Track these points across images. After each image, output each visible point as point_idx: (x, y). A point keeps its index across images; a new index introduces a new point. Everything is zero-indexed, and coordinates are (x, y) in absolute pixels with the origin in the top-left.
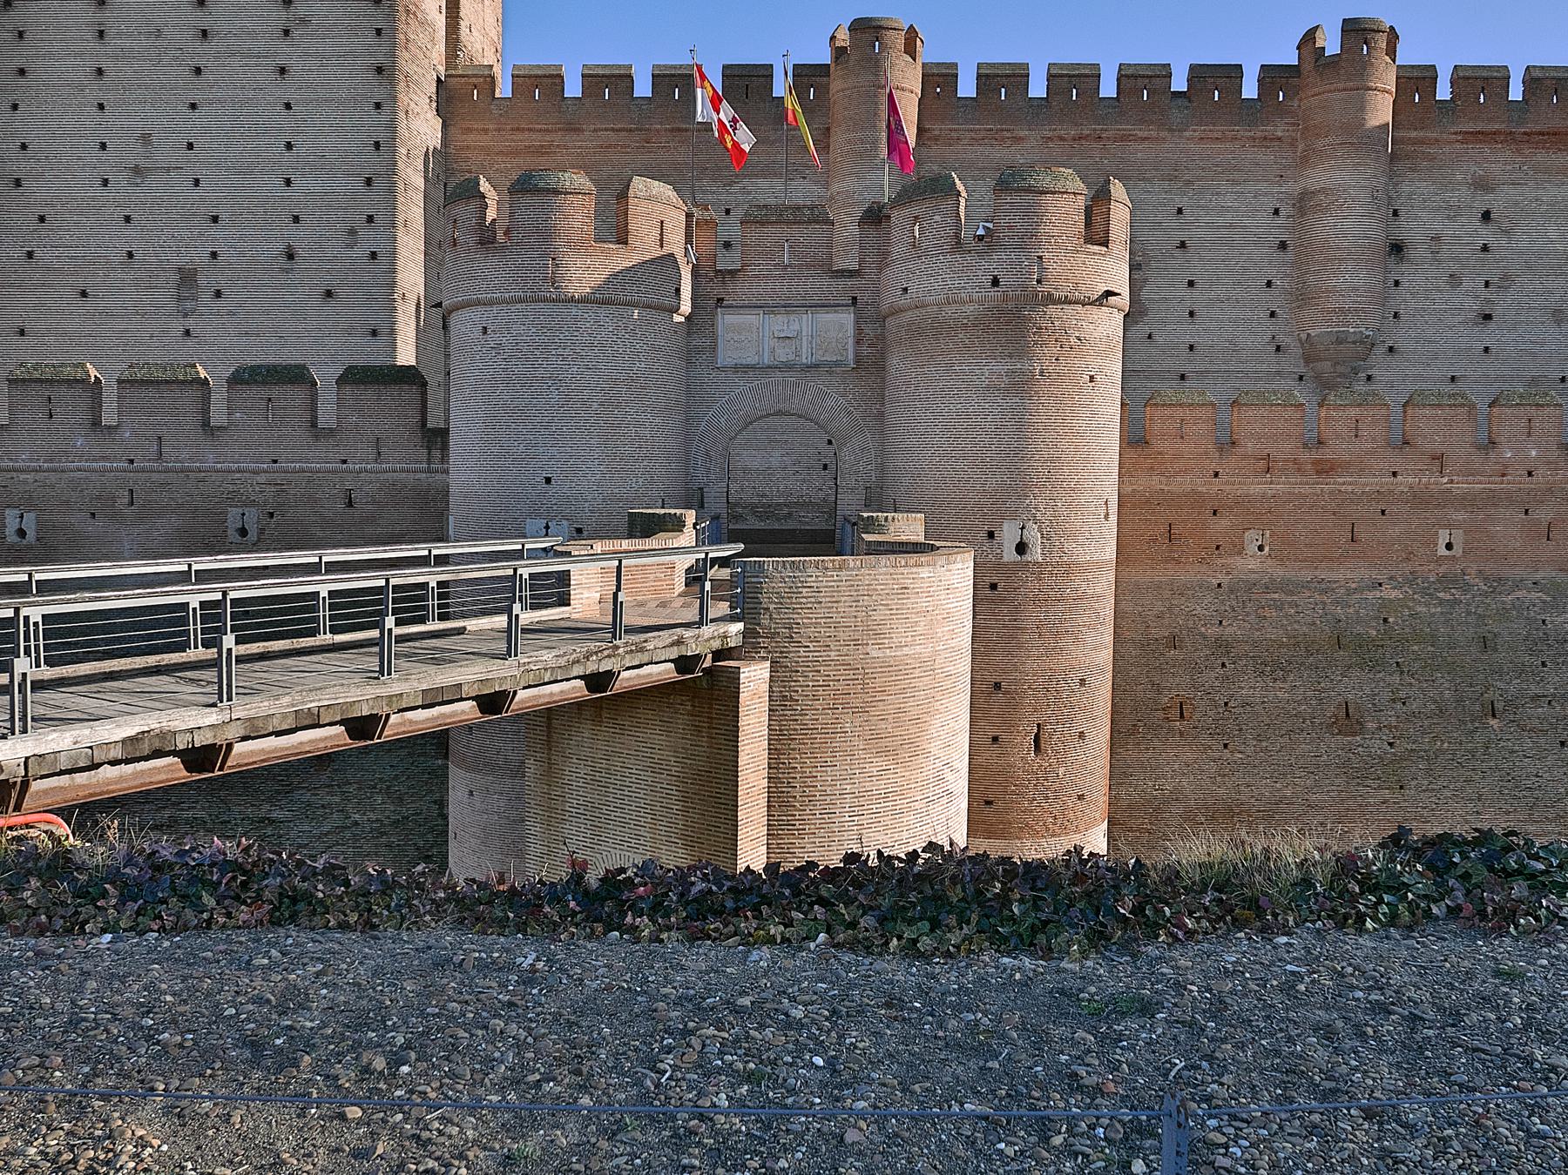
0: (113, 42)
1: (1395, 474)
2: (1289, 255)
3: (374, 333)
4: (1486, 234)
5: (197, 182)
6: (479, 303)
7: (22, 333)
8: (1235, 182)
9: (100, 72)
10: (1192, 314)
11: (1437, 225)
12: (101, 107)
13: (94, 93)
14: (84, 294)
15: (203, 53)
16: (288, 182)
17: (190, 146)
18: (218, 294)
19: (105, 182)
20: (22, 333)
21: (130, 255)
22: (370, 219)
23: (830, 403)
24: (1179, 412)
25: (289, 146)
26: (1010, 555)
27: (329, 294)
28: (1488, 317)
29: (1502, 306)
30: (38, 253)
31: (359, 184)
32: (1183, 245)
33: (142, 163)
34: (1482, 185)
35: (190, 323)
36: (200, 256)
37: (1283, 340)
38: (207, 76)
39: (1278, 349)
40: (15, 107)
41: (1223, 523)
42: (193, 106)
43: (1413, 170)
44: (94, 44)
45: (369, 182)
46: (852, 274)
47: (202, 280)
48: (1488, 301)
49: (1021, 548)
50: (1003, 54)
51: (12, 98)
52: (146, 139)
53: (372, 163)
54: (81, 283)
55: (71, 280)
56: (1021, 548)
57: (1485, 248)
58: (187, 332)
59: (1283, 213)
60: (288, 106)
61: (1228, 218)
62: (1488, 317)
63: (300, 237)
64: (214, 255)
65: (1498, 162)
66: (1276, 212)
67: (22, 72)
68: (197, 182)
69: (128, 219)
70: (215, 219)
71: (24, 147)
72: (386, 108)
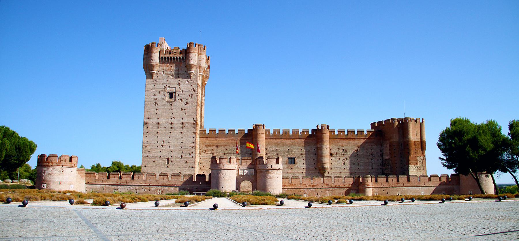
0: (160, 129)
1: (322, 187)
2: (316, 156)
3: (192, 167)
5: (170, 147)
6: (215, 169)
7: (145, 166)
8: (309, 145)
9: (158, 132)
11: (337, 151)
12: (158, 137)
15: (171, 130)
16: (182, 147)
17: (169, 142)
19: (158, 147)
20: (145, 166)
21: (160, 156)
22: (192, 152)
23: (251, 179)
24: (295, 179)
28: (344, 164)
30: (148, 156)
31: (191, 147)
33: (163, 144)
34: (342, 146)
36: (170, 157)
37: (316, 168)
38: (172, 133)
39: (316, 169)
40: (146, 137)
42: (170, 137)
43: (333, 144)
45: (192, 147)
46: (254, 165)
47: (170, 160)
48: (344, 162)
50: (276, 128)
51: (146, 136)
52: (163, 141)
53: (193, 145)
54: (154, 160)
55: (152, 159)
57: (343, 154)
58: (167, 167)
59: (315, 150)
60: (182, 137)
63: (183, 154)
64: (171, 157)
65: (344, 143)
66: (314, 150)
67: (148, 132)
68: (170, 147)
69: (160, 152)
70: (172, 152)
72: (195, 138)
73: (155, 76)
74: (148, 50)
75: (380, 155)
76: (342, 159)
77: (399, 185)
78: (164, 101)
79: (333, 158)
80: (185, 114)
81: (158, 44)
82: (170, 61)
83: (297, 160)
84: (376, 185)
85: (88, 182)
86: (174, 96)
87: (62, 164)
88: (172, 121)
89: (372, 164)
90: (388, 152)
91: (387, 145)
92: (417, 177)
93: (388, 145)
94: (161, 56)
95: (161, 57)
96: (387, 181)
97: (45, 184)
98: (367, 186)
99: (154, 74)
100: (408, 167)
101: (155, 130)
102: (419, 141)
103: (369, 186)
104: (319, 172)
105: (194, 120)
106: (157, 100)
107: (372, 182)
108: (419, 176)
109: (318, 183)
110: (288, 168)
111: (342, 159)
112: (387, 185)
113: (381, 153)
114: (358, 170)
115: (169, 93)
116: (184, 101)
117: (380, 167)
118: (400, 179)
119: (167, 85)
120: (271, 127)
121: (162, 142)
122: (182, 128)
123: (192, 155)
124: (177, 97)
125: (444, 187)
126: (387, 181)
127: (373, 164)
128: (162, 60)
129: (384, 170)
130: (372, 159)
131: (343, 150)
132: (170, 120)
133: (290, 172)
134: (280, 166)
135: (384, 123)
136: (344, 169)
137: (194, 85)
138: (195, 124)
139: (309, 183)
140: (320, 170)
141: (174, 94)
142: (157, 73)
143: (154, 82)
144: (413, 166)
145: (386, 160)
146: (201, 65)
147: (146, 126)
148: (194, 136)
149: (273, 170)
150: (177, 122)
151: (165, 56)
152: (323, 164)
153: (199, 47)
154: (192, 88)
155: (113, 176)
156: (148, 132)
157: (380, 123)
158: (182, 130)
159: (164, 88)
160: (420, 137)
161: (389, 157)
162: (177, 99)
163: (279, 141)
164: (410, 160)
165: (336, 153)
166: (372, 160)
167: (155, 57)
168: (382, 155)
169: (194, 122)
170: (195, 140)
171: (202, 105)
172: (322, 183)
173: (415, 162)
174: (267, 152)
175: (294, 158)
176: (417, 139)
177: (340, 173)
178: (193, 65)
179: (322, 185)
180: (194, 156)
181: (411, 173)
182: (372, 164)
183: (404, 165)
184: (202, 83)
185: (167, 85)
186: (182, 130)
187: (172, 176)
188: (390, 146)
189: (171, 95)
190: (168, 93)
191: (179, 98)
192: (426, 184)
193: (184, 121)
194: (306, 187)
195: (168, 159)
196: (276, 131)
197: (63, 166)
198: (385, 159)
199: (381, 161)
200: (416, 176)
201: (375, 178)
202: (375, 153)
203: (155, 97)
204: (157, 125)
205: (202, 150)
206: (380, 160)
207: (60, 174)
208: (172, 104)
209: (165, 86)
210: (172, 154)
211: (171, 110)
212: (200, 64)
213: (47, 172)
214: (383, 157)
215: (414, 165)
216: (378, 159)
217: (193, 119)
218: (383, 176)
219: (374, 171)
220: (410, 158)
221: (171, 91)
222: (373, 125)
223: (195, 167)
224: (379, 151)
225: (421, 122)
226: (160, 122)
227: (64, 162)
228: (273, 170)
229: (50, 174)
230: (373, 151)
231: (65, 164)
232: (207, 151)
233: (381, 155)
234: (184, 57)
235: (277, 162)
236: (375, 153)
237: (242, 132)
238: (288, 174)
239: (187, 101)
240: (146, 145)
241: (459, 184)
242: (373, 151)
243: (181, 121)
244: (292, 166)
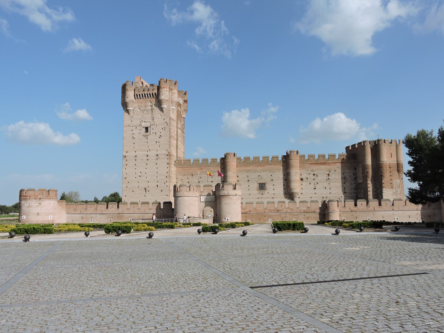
3: (167, 195)
4: (314, 177)
10: (274, 189)
11: (307, 176)
13: (135, 167)
14: (133, 191)
15: (147, 162)
18: (149, 191)
19: (136, 178)
22: (167, 181)
25: (157, 173)
26: (227, 220)
27: (162, 191)
28: (315, 189)
29: (317, 186)
31: (165, 177)
32: (272, 180)
33: (140, 175)
34: (313, 171)
35: (145, 195)
36: (146, 186)
38: (148, 165)
41: (266, 218)
43: (303, 169)
44: (135, 161)
45: (166, 177)
49: (228, 220)
51: (125, 168)
53: (167, 175)
56: (228, 220)
57: (314, 179)
61: (278, 176)
62: (315, 189)
63: (158, 184)
65: (315, 167)
71: (127, 174)
73: (131, 113)
74: (124, 88)
75: (353, 179)
76: (313, 184)
77: (369, 209)
78: (141, 135)
79: (303, 183)
80: (159, 146)
81: (132, 82)
82: (144, 97)
83: (268, 186)
84: (343, 209)
85: (68, 212)
86: (149, 130)
87: (40, 197)
88: (148, 153)
89: (345, 188)
90: (361, 175)
91: (360, 168)
92: (390, 201)
93: (361, 168)
94: (136, 93)
95: (135, 95)
96: (356, 205)
97: (25, 215)
98: (333, 210)
99: (130, 110)
100: (382, 190)
101: (133, 163)
102: (394, 164)
103: (335, 210)
104: (289, 197)
105: (168, 151)
106: (134, 134)
107: (338, 206)
108: (392, 200)
109: (283, 208)
110: (259, 193)
111: (313, 184)
112: (355, 208)
113: (354, 177)
114: (330, 194)
115: (144, 128)
116: (158, 134)
117: (353, 191)
118: (358, 203)
119: (142, 121)
120: (242, 155)
121: (140, 173)
122: (157, 159)
123: (167, 184)
124: (152, 131)
125: (426, 211)
126: (356, 205)
127: (346, 188)
128: (136, 96)
129: (357, 194)
130: (344, 183)
131: (314, 174)
132: (146, 153)
133: (261, 198)
134: (238, 192)
135: (357, 146)
136: (315, 193)
137: (166, 119)
138: (169, 155)
139: (273, 209)
140: (290, 195)
141: (149, 128)
142: (133, 110)
143: (130, 118)
144: (387, 189)
145: (360, 184)
146: (173, 100)
147: (125, 159)
148: (168, 166)
149: (229, 195)
150: (152, 154)
151: (140, 93)
152: (291, 189)
153: (170, 83)
154: (165, 121)
155: (90, 206)
156: (127, 165)
157: (353, 146)
158: (157, 161)
159: (140, 123)
160: (396, 159)
161: (362, 180)
162: (151, 133)
163: (251, 168)
164: (383, 183)
165: (307, 178)
166: (345, 184)
167: (130, 95)
168: (356, 179)
169: (168, 153)
170: (169, 170)
171: (177, 137)
172: (287, 208)
173: (390, 185)
174: (239, 179)
175: (265, 184)
176: (393, 161)
177: (311, 197)
178: (164, 100)
179: (287, 210)
180: (168, 185)
181: (385, 197)
182: (345, 188)
183: (378, 189)
184: (177, 117)
185: (142, 121)
186: (157, 161)
187: (152, 204)
188: (362, 169)
189: (147, 129)
190: (143, 127)
191: (154, 131)
192: (401, 209)
193: (158, 153)
194: (271, 212)
195: (145, 189)
196: (247, 159)
197: (40, 199)
198: (358, 183)
199: (354, 185)
200: (388, 200)
201: (354, 202)
202: (348, 177)
203: (132, 132)
204: (135, 158)
205: (178, 179)
206: (354, 183)
207: (37, 206)
208: (147, 138)
209: (141, 121)
210: (149, 184)
211: (146, 143)
212: (172, 99)
213: (26, 205)
214: (357, 180)
215: (390, 188)
216: (351, 183)
217: (167, 150)
218: (350, 200)
219: (346, 195)
220: (383, 181)
221: (146, 126)
222: (347, 148)
223: (169, 195)
224: (352, 174)
225: (398, 143)
226: (137, 155)
227: (41, 195)
228: (229, 195)
229: (29, 206)
230: (345, 175)
231: (43, 197)
232: (184, 180)
233: (354, 178)
234: (157, 93)
235: (235, 189)
236: (348, 177)
237: (215, 160)
238: (259, 199)
239: (161, 134)
240: (125, 176)
241: (441, 208)
242: (345, 175)
243: (155, 153)
244: (262, 191)
